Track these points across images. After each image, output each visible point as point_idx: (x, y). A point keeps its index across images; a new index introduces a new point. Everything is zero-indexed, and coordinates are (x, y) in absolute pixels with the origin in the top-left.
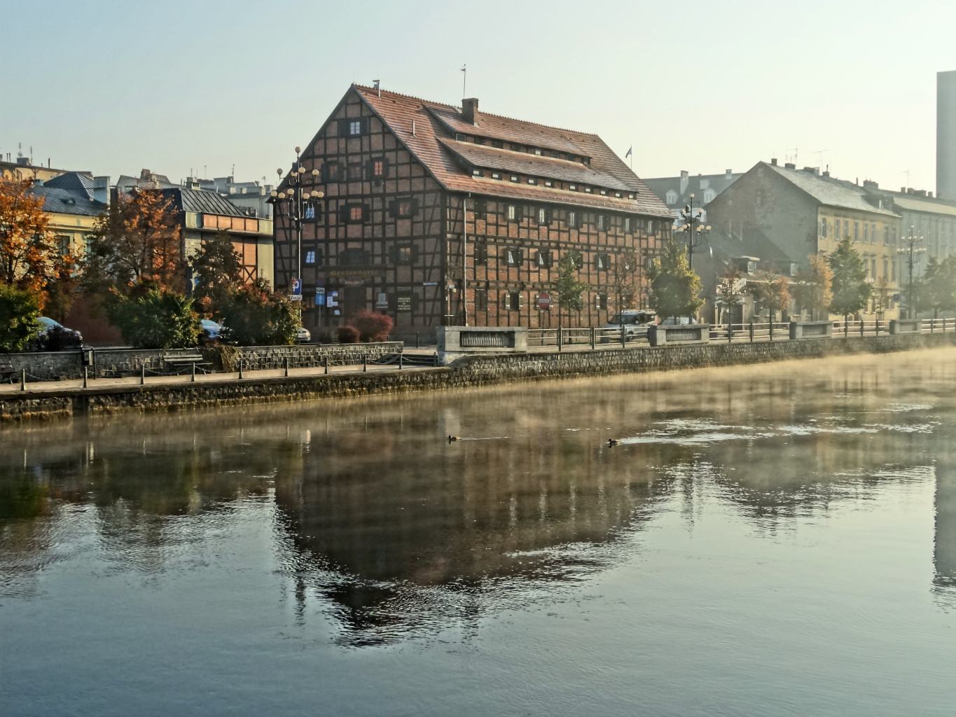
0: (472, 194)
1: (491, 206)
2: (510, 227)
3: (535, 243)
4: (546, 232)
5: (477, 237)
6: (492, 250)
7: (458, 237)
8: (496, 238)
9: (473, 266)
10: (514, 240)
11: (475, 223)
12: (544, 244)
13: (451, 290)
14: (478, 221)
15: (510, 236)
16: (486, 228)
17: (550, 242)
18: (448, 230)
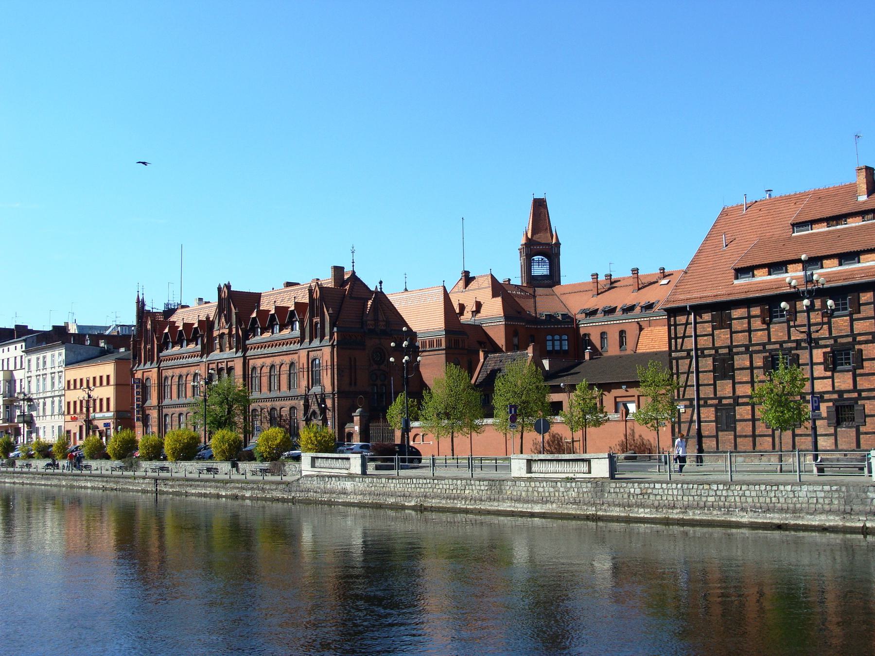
0: (690, 306)
1: (736, 313)
2: (771, 330)
3: (822, 343)
4: (848, 323)
5: (716, 349)
6: (742, 361)
7: (689, 354)
8: (747, 347)
9: (712, 382)
10: (781, 343)
11: (712, 335)
12: (839, 340)
13: (679, 410)
14: (716, 332)
15: (772, 340)
16: (731, 337)
17: (854, 336)
18: (673, 348)
